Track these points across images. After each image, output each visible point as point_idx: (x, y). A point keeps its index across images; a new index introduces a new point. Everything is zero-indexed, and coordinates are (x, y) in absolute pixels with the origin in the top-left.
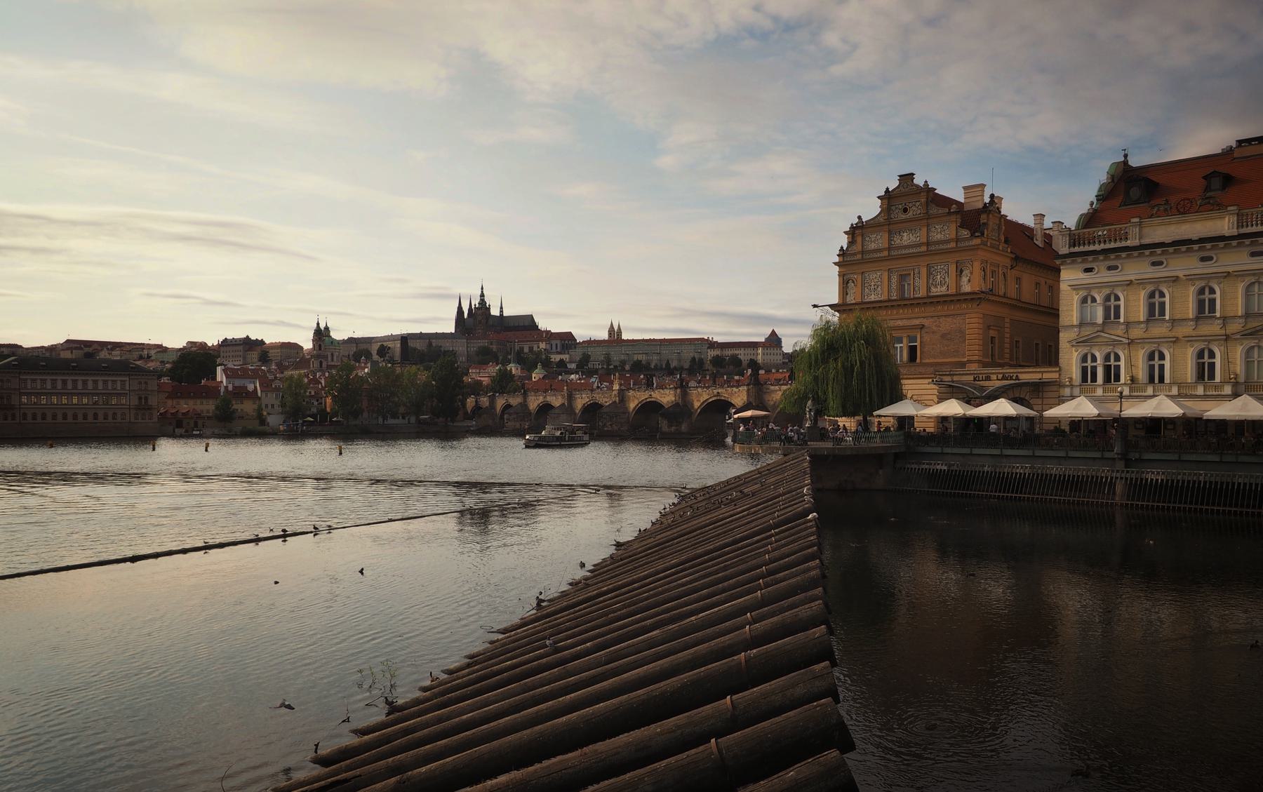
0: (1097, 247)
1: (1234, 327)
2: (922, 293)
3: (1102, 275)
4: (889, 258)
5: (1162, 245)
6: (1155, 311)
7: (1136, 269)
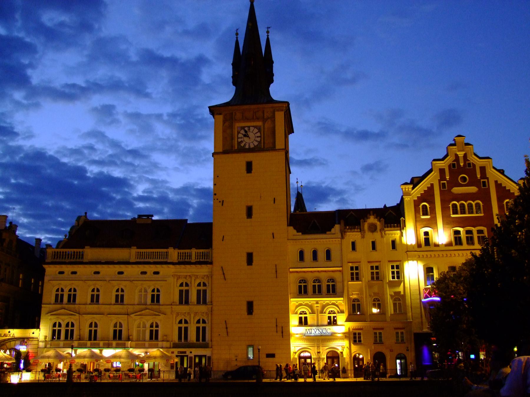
6: (95, 299)
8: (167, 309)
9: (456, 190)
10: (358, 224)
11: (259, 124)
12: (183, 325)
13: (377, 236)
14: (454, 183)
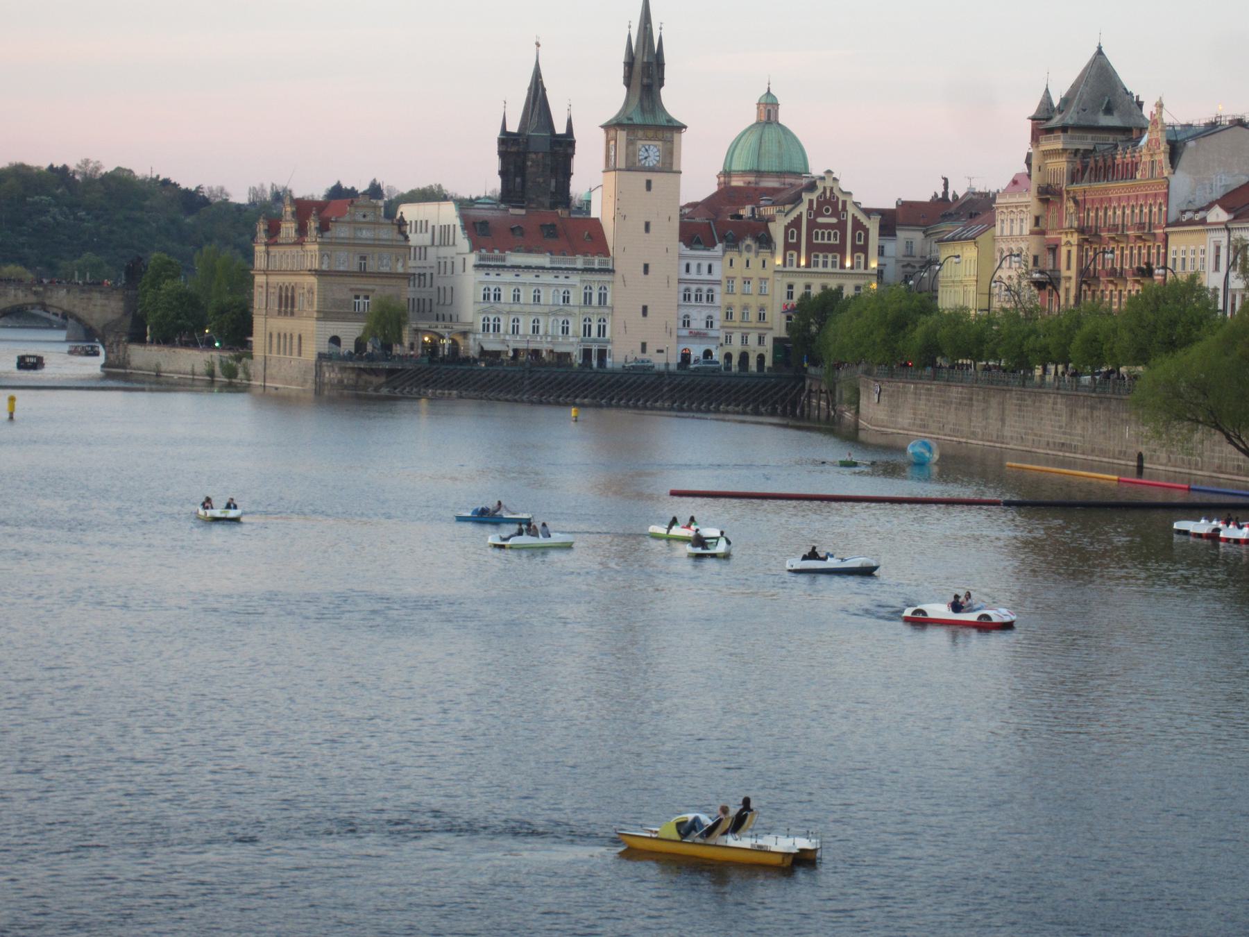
0: (492, 263)
1: (546, 310)
2: (375, 269)
3: (492, 277)
4: (354, 245)
5: (519, 267)
6: (517, 298)
7: (508, 276)
8: (576, 311)
9: (820, 220)
10: (737, 246)
11: (659, 143)
12: (587, 323)
13: (751, 256)
14: (819, 213)
